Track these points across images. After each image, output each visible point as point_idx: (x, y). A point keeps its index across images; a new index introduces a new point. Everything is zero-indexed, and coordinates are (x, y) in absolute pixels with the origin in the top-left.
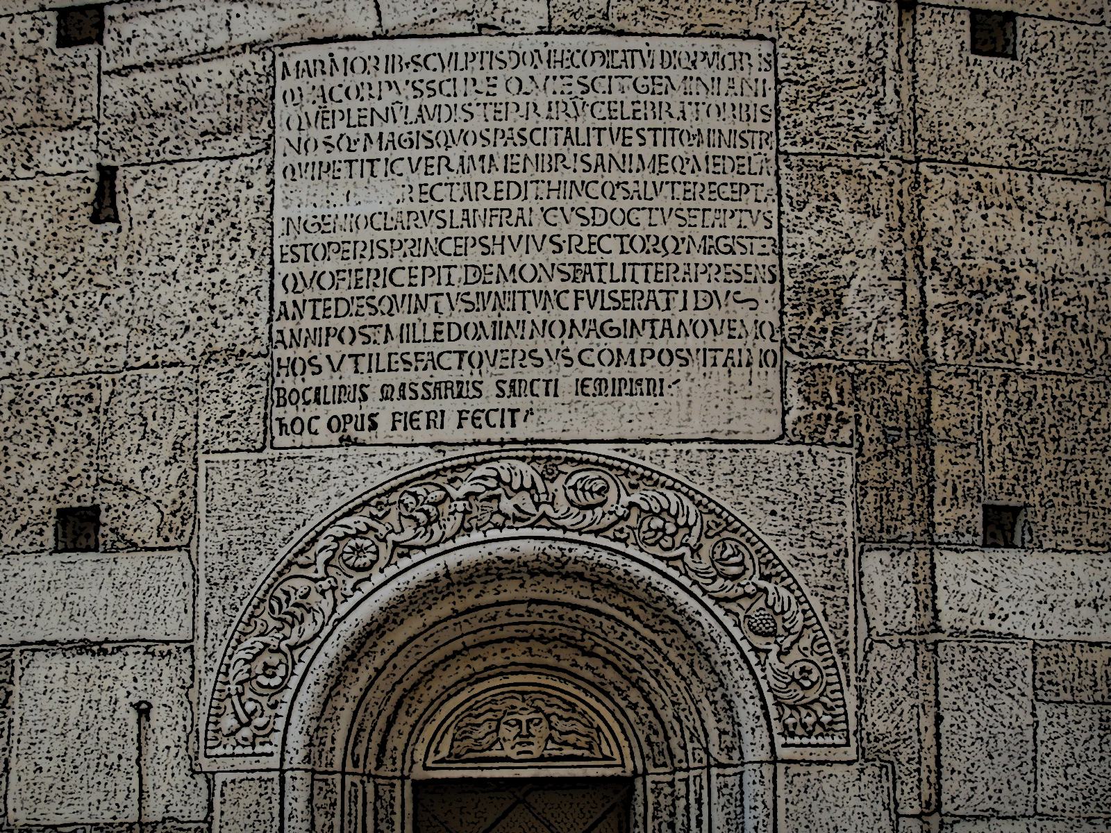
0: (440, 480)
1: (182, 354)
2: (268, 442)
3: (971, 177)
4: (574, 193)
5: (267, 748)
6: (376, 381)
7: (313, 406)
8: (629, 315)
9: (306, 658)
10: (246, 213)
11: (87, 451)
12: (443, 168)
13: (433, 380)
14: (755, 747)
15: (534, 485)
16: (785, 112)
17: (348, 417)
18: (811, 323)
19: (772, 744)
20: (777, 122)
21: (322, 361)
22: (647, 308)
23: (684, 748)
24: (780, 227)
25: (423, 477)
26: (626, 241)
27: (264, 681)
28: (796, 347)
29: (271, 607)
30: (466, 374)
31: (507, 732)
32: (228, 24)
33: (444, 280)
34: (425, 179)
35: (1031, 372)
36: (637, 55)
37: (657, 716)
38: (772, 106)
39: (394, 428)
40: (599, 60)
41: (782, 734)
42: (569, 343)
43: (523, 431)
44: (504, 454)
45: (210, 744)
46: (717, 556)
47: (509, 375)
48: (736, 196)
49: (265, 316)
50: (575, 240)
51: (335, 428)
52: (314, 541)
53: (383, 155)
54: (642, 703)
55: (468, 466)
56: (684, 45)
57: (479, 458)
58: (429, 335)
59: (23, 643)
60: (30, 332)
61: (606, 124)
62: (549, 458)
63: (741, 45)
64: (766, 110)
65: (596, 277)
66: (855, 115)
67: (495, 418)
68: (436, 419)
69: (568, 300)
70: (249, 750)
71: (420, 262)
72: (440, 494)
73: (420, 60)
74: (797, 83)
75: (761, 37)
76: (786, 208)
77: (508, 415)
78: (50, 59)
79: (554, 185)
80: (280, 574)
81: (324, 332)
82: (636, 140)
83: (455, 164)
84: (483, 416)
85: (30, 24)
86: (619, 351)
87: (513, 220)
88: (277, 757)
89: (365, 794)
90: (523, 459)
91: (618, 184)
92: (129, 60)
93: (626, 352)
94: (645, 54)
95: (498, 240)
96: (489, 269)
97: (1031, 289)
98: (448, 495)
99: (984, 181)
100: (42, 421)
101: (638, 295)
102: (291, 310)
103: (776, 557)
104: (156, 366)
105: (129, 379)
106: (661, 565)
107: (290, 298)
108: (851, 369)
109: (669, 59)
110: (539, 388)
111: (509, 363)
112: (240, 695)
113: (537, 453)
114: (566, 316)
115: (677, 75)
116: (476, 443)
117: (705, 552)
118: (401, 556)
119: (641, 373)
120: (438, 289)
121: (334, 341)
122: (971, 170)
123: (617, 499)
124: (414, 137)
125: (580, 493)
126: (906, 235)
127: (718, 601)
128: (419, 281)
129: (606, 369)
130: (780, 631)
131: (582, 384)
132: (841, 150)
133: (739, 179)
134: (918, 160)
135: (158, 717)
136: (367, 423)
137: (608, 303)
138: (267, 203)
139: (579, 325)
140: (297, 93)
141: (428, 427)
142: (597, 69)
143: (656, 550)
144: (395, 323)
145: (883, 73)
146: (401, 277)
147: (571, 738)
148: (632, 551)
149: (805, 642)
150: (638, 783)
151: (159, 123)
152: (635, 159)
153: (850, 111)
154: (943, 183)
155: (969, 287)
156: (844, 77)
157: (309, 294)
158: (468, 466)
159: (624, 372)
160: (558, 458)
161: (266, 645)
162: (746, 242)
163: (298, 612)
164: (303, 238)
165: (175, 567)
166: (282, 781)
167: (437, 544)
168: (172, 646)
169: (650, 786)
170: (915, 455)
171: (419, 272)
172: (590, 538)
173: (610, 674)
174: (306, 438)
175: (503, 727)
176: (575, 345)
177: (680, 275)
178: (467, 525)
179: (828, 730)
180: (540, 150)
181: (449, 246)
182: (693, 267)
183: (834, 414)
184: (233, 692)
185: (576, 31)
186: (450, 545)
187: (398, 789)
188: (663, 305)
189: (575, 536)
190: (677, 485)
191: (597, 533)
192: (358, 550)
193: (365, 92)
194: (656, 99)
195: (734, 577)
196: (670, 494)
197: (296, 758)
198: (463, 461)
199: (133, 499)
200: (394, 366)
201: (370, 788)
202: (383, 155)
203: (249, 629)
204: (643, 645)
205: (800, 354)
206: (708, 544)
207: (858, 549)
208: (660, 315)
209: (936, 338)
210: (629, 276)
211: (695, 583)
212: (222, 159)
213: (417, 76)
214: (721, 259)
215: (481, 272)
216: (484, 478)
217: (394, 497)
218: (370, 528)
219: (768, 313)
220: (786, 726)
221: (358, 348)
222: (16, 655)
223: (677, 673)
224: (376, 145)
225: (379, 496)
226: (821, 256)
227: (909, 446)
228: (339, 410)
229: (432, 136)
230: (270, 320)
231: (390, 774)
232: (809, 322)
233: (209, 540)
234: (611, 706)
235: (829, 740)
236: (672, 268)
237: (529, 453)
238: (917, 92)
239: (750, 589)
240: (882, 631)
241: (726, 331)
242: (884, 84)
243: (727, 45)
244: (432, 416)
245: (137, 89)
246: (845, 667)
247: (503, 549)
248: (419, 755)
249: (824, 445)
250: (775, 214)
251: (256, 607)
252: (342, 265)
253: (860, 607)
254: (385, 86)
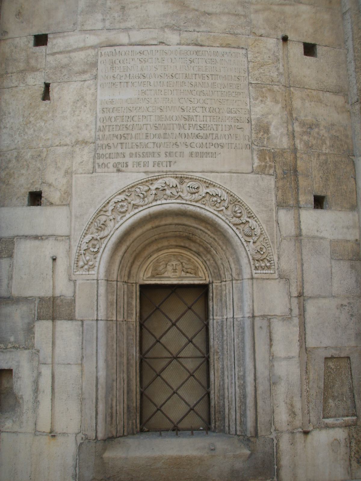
0: (147, 184)
1: (68, 142)
2: (94, 171)
3: (306, 92)
4: (188, 94)
5: (93, 272)
6: (127, 152)
7: (108, 159)
8: (205, 132)
9: (105, 242)
10: (88, 98)
11: (38, 173)
12: (149, 85)
13: (145, 152)
14: (246, 274)
15: (176, 185)
16: (250, 71)
17: (119, 163)
18: (260, 136)
19: (252, 273)
20: (248, 74)
21: (111, 145)
22: (210, 130)
23: (224, 274)
24: (250, 106)
25: (142, 183)
26: (204, 109)
27: (92, 250)
28: (256, 143)
29: (95, 225)
30: (156, 150)
31: (169, 268)
32: (84, 40)
33: (149, 120)
34: (143, 88)
35: (326, 153)
36: (206, 52)
37: (216, 263)
38: (247, 69)
39: (133, 167)
40: (195, 54)
41: (255, 269)
42: (187, 140)
43: (173, 168)
44: (167, 176)
45: (75, 270)
46: (234, 210)
47: (168, 150)
48: (237, 96)
49: (94, 130)
50: (188, 108)
51: (115, 166)
52: (108, 203)
53: (130, 81)
54: (211, 259)
55: (156, 179)
56: (220, 50)
57: (160, 177)
58: (144, 137)
59: (17, 236)
60: (22, 135)
61: (198, 72)
62: (181, 177)
63: (237, 50)
64: (245, 70)
65: (195, 120)
66: (271, 72)
67: (164, 164)
68: (146, 164)
69: (187, 127)
70: (87, 273)
71: (141, 114)
72: (147, 188)
73: (142, 52)
74: (254, 62)
75: (242, 48)
76: (252, 100)
77: (168, 163)
78: (31, 50)
79: (182, 91)
80: (97, 214)
81: (112, 135)
82: (206, 78)
83: (152, 84)
84: (160, 163)
85: (25, 40)
86: (202, 143)
87: (170, 101)
88: (96, 275)
89: (124, 289)
90: (173, 177)
91: (201, 91)
92: (55, 51)
93: (204, 144)
94: (209, 52)
97: (325, 127)
98: (150, 189)
99: (310, 94)
100: (25, 163)
101: (208, 126)
102: (102, 128)
103: (252, 211)
104: (60, 146)
105: (52, 150)
106: (216, 213)
107: (101, 125)
108: (273, 151)
109: (216, 54)
110: (178, 154)
112: (84, 254)
113: (178, 176)
115: (218, 59)
116: (159, 172)
117: (230, 208)
118: (135, 208)
119: (209, 150)
120: (147, 123)
121: (115, 138)
122: (306, 90)
123: (203, 191)
124: (140, 75)
125: (191, 188)
126: (288, 110)
127: (234, 225)
128: (141, 120)
129: (198, 149)
130: (254, 235)
131: (191, 154)
132: (267, 83)
133: (238, 91)
134: (290, 87)
135: (59, 261)
136: (125, 165)
137: (199, 128)
138: (94, 95)
139: (190, 135)
140: (105, 61)
141: (144, 166)
142: (194, 56)
143: (215, 208)
144: (134, 133)
145: (279, 60)
146: (136, 119)
147: (189, 270)
148: (207, 208)
149: (261, 239)
150: (210, 286)
151: (63, 70)
152: (206, 84)
153: (270, 71)
154: (297, 93)
155: (307, 126)
156: (268, 61)
157: (107, 124)
158: (156, 179)
159: (204, 150)
160: (184, 177)
161: (93, 238)
162: (240, 110)
163: (103, 226)
164: (106, 106)
165: (65, 209)
166: (98, 283)
167: (146, 205)
168: (63, 238)
169: (214, 286)
170: (293, 179)
171: (141, 117)
172: (194, 204)
173: (201, 249)
174: (106, 169)
175: (168, 266)
176: (189, 141)
177: (220, 120)
178: (156, 199)
179: (269, 268)
180: (178, 80)
181: (150, 109)
182: (224, 117)
183: (268, 165)
184: (82, 253)
185: (188, 45)
186: (150, 205)
187: (135, 287)
188: (215, 129)
189: (190, 203)
190: (221, 187)
191: (197, 202)
192: (122, 206)
193: (125, 62)
194: (213, 65)
195: (239, 217)
196: (218, 190)
197: (102, 275)
198: (155, 178)
199: (52, 189)
200: (133, 147)
201: (126, 286)
202: (130, 81)
203: (88, 232)
204: (211, 239)
205: (257, 146)
206: (230, 206)
207: (277, 208)
208: (215, 132)
209: (297, 142)
210: (205, 120)
211: (227, 219)
212: (82, 81)
213: (141, 57)
215: (160, 118)
216: (161, 183)
217: (133, 189)
218: (126, 199)
219: (247, 132)
220: (256, 267)
221: (123, 141)
222: (15, 240)
223: (222, 249)
224: (128, 78)
225: (128, 189)
226: (263, 115)
227: (291, 175)
228: (116, 160)
229: (145, 75)
230: (95, 132)
231: (132, 282)
232: (260, 135)
233: (75, 203)
234: (202, 260)
235: (269, 272)
236: (218, 118)
237: (175, 175)
238: (289, 66)
239: (244, 221)
240: (285, 236)
241: (235, 138)
242: (279, 63)
243: (233, 50)
244: (145, 163)
245: (57, 59)
246: (274, 248)
247: (167, 207)
248: (141, 276)
249: (265, 175)
250: (248, 102)
251: (90, 225)
252: (118, 114)
253: (278, 228)
254: (131, 60)
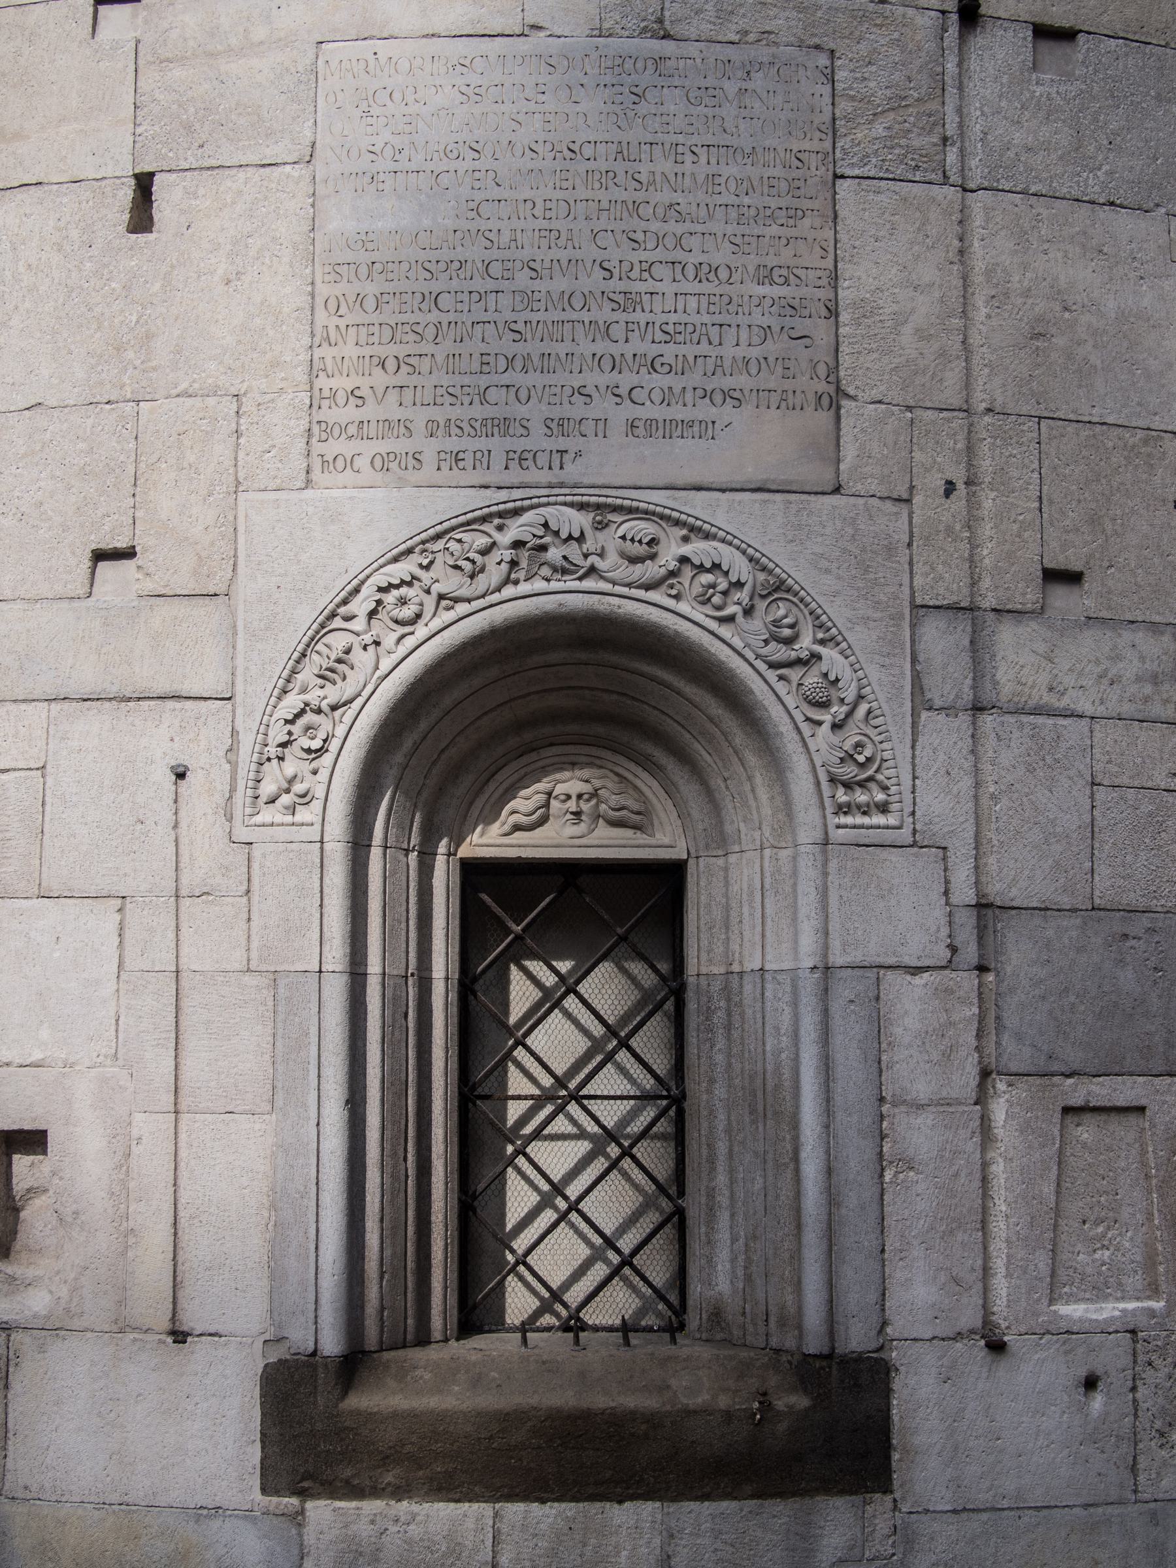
8: (682, 350)
47: (556, 412)
48: (791, 222)
84: (530, 456)
93: (676, 391)
95: (547, 264)
96: (537, 296)
101: (690, 328)
111: (556, 400)
114: (615, 350)
133: (795, 203)
177: (732, 308)
214: (776, 291)
241: (779, 369)
